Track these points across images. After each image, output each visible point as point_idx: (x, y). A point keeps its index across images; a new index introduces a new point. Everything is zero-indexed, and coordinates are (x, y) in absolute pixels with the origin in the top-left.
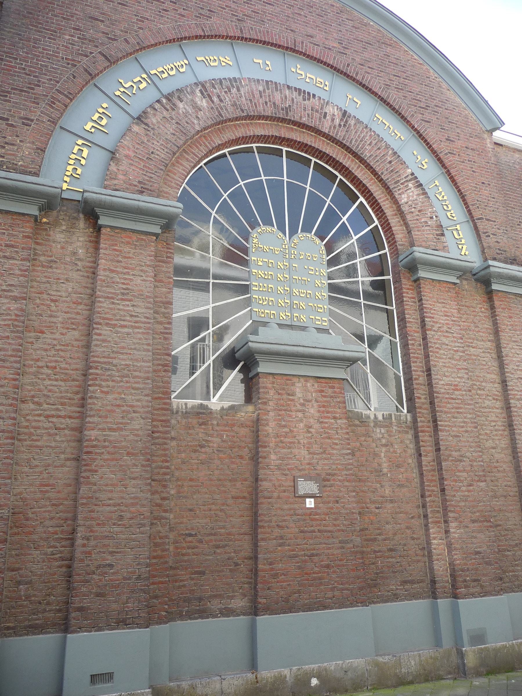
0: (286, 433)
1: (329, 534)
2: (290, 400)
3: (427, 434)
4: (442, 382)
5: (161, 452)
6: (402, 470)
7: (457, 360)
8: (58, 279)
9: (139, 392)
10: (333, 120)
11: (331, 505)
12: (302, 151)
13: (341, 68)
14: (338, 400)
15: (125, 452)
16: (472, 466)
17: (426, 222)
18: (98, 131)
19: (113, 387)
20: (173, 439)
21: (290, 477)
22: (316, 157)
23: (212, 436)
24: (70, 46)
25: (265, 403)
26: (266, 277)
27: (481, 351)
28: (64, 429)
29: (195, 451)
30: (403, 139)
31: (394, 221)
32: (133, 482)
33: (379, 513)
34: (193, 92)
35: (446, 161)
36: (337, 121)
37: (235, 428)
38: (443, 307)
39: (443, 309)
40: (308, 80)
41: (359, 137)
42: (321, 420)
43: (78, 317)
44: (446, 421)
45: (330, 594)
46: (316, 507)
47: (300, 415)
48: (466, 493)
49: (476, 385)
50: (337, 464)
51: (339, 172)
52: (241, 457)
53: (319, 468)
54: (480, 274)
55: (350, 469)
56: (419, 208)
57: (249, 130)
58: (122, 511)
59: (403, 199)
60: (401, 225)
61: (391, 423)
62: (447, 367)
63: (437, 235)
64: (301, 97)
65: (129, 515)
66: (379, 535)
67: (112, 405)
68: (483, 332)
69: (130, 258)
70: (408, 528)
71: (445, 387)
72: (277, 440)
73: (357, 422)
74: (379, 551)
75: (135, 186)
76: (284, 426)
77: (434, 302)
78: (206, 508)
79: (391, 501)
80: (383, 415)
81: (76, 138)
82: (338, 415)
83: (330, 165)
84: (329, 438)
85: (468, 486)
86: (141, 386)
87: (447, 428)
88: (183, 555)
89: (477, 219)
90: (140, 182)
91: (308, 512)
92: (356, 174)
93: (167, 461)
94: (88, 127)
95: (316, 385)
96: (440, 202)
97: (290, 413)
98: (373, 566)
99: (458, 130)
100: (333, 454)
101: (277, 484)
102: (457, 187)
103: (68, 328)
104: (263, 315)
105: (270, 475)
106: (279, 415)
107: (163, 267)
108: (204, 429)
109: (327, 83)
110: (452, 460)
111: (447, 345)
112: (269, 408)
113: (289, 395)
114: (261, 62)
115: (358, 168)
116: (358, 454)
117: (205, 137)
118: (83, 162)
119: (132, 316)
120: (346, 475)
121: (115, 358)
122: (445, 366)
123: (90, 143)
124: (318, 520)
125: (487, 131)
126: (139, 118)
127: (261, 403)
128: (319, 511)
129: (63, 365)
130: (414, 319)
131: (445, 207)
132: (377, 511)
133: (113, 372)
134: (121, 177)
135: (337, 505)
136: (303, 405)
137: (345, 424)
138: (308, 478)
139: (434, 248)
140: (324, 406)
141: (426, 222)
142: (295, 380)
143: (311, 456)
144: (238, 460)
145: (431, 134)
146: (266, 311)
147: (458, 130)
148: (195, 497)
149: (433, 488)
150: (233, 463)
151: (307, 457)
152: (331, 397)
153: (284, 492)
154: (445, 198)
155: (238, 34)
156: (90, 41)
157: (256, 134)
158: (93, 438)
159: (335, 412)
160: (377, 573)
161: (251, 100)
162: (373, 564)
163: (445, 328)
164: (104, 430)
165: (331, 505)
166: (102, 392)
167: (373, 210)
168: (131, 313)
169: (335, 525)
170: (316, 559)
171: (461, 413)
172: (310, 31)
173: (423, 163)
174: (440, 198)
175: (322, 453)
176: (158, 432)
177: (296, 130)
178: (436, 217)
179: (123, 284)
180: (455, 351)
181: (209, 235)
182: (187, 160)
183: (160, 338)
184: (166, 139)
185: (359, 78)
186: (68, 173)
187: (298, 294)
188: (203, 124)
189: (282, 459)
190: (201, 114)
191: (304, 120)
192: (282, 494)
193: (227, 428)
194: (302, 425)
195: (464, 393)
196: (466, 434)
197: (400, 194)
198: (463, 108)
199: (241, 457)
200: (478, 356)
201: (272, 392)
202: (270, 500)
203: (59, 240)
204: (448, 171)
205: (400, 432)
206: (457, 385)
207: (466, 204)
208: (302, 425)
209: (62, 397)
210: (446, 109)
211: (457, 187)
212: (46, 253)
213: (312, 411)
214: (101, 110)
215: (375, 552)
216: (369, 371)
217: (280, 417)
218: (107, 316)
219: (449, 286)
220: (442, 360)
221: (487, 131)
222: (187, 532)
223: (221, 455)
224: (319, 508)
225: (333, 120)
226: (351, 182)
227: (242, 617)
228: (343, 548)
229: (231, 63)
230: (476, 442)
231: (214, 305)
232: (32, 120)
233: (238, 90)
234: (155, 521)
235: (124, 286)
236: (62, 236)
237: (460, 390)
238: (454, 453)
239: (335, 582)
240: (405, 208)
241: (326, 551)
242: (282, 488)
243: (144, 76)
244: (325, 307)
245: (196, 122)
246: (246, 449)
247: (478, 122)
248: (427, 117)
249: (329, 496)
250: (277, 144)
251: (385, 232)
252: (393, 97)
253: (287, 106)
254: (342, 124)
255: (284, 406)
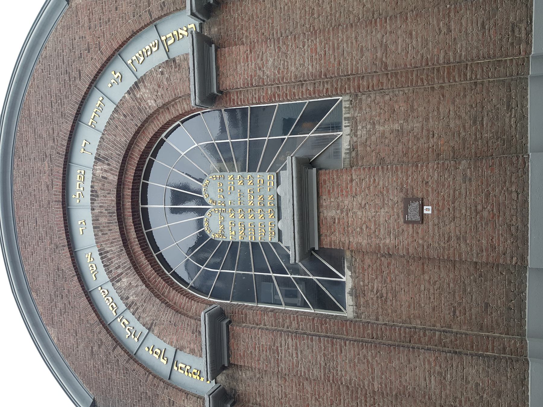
0: (367, 227)
1: (457, 193)
2: (339, 222)
3: (361, 82)
4: (310, 67)
5: (388, 333)
6: (396, 107)
7: (287, 48)
8: (270, 391)
9: (343, 349)
10: (106, 171)
11: (430, 189)
12: (138, 192)
13: (63, 160)
14: (335, 177)
15: (389, 364)
16: (391, 32)
17: (167, 79)
18: (165, 356)
19: (341, 367)
20: (377, 319)
21: (405, 226)
22: (140, 180)
23: (373, 287)
24: (115, 371)
25: (344, 244)
26: (243, 228)
27: (275, 11)
28: (374, 399)
29: (386, 301)
30: (101, 99)
31: (174, 112)
32: (411, 361)
33: (438, 135)
34: (120, 288)
35: (108, 53)
36: (106, 167)
37: (366, 267)
38: (240, 63)
39: (242, 64)
40: (82, 189)
41: (113, 147)
42: (354, 194)
43: (294, 380)
44: (347, 64)
45: (514, 195)
46: (432, 205)
47: (350, 214)
48: (419, 40)
49: (309, 19)
50: (392, 181)
51: (146, 158)
52: (389, 264)
53: (396, 199)
54: (201, 18)
55: (397, 168)
56: (156, 87)
57: (135, 242)
58: (434, 372)
59: (152, 104)
60: (176, 103)
61: (354, 118)
62: (295, 60)
63: (176, 68)
64: (96, 198)
65: (437, 368)
66: (459, 134)
67: (355, 370)
68: (257, 9)
69: (247, 345)
70: (453, 103)
71: (314, 64)
72: (373, 236)
73: (354, 154)
74: (476, 135)
75: (196, 336)
76: (361, 229)
77: (237, 74)
78: (432, 298)
79: (427, 120)
80: (346, 126)
81: (173, 370)
82: (349, 178)
83: (143, 168)
84: (369, 188)
85: (412, 38)
86: (338, 347)
87: (354, 63)
88: (471, 319)
89: (152, 18)
90: (193, 333)
91: (436, 212)
92: (144, 148)
93: (395, 329)
94: (165, 362)
95: (324, 197)
96: (146, 58)
97: (350, 222)
98: (490, 143)
99: (77, 38)
100: (384, 184)
101: (410, 240)
102: (128, 39)
103: (303, 389)
104: (273, 233)
105: (403, 245)
106: (352, 232)
107: (249, 317)
108: (368, 292)
109: (79, 171)
110: (386, 57)
111: (274, 59)
112: (347, 242)
113: (334, 223)
114: (81, 229)
115: (138, 146)
116: (382, 155)
117: (149, 278)
118: (188, 367)
119: (288, 348)
120: (402, 172)
121: (320, 364)
122: (295, 64)
123: (175, 362)
124: (443, 204)
125: (68, 4)
126: (149, 329)
127: (344, 248)
128: (435, 202)
129: (329, 394)
130: (255, 94)
131: (149, 53)
132: (436, 135)
133: (331, 366)
134: (192, 346)
135: (430, 183)
136: (342, 212)
137: (355, 170)
138: (406, 212)
139: (187, 72)
140: (342, 191)
141: (167, 79)
142: (322, 217)
143: (385, 205)
144: (392, 267)
145: (90, 70)
146: (270, 230)
147: (77, 38)
148: (423, 305)
149: (414, 76)
150: (394, 271)
151: (386, 210)
152: (333, 183)
153: (418, 233)
154: (140, 52)
155: (66, 249)
156: (107, 357)
157: (135, 236)
158: (380, 386)
159: (347, 180)
160: (497, 139)
161: (112, 243)
162: (487, 142)
163: (259, 61)
164: (373, 378)
165: (430, 189)
166: (346, 375)
167: (169, 127)
168: (286, 349)
169: (449, 186)
170: (479, 207)
171: (338, 44)
172: (44, 187)
173: (116, 76)
174: (142, 58)
175: (383, 195)
176: (372, 335)
177: (123, 202)
178: (160, 67)
179: (266, 351)
180: (279, 50)
181: (220, 272)
182: (169, 292)
183: (302, 325)
184: (158, 311)
185: (65, 143)
186: (198, 378)
187: (252, 202)
188: (140, 283)
189: (389, 233)
190: (134, 283)
191: (113, 197)
192: (420, 235)
193: (366, 274)
194: (359, 213)
195: (318, 40)
196: (359, 38)
197: (149, 107)
198: (56, 31)
199: (389, 264)
200: (280, 16)
201: (333, 238)
202: (425, 247)
203: (244, 388)
204: (116, 50)
205: (361, 108)
206: (311, 49)
207: (140, 30)
208: (359, 213)
209: (352, 398)
210: (63, 52)
211: (128, 39)
212: (254, 397)
213: (346, 202)
214: (151, 352)
215: (476, 140)
216: (308, 135)
217: (354, 232)
218: (291, 365)
219: (219, 56)
220: (289, 66)
221: (68, 4)
222: (452, 314)
223: (388, 281)
224: (433, 200)
225: (106, 171)
226: (151, 148)
227: (527, 275)
228: (470, 180)
229: (90, 254)
230: (366, 26)
231: (271, 272)
232: (169, 399)
233: (107, 252)
234: (443, 344)
235: (268, 351)
236: (240, 385)
237: (315, 45)
238: (379, 55)
239: (502, 189)
240: (160, 102)
241: (473, 197)
242: (415, 235)
243: (119, 320)
244: (258, 176)
245: (140, 288)
246: (383, 259)
247: (63, 14)
248: (75, 74)
249: (422, 191)
250: (139, 214)
251: (185, 116)
252: (71, 111)
253: (106, 212)
254: (106, 162)
255: (344, 228)
